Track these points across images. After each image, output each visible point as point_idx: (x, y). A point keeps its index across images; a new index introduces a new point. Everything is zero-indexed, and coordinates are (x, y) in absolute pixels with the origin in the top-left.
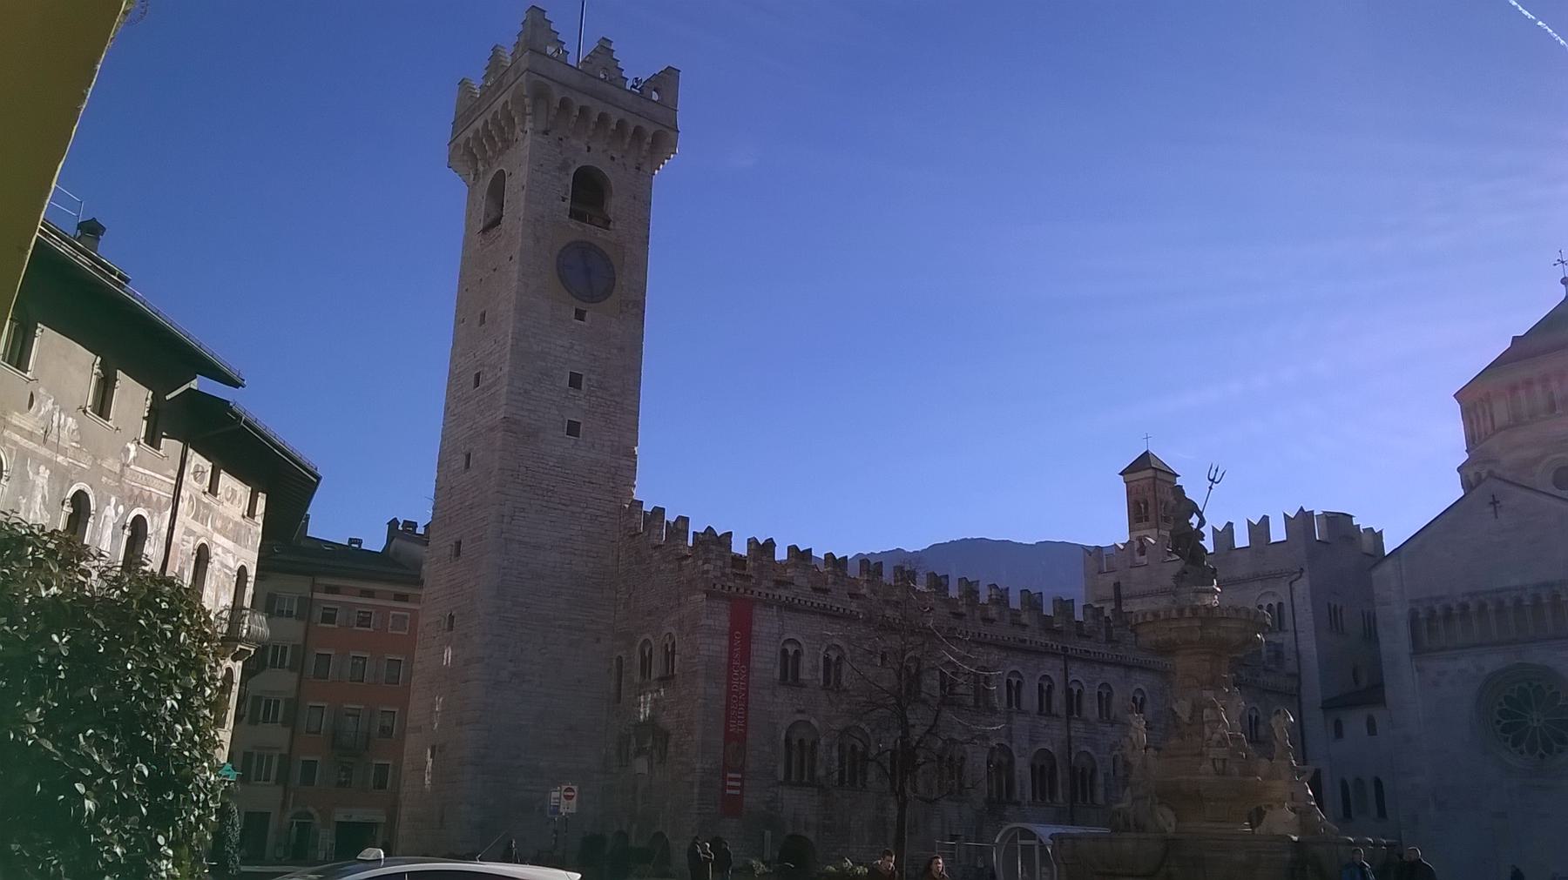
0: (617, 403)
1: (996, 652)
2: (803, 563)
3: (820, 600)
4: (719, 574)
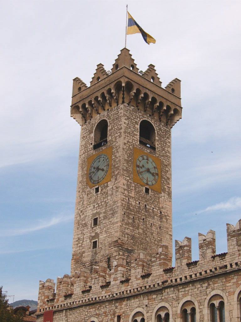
0: (111, 222)
1: (199, 286)
2: (79, 279)
4: (42, 304)
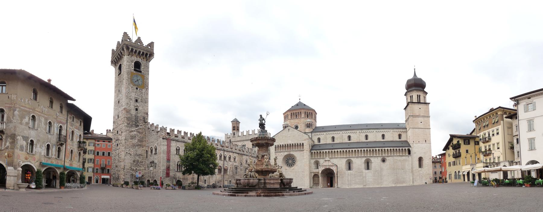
3: (183, 140)
